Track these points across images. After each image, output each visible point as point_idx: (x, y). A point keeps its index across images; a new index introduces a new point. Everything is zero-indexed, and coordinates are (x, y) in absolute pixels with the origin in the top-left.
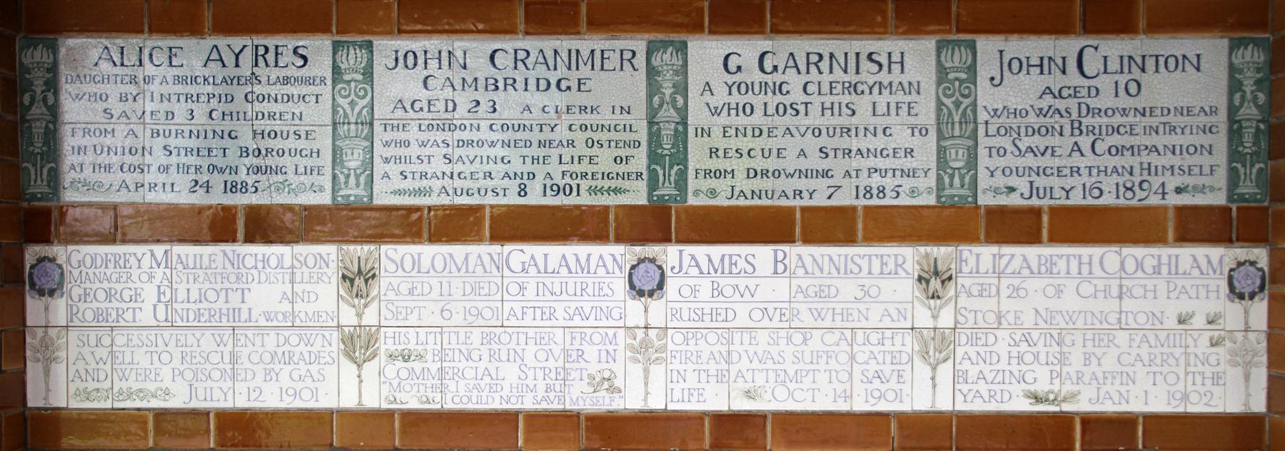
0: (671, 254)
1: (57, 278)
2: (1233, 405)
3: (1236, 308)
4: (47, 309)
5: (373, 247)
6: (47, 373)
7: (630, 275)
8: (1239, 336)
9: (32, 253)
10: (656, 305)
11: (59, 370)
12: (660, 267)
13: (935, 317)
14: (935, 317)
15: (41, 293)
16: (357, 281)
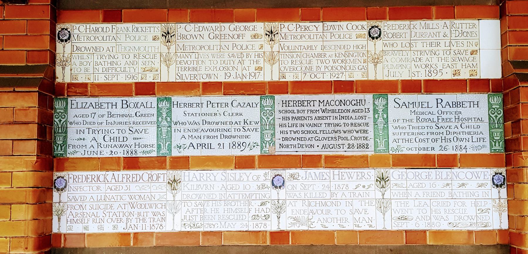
0: (286, 173)
1: (64, 184)
2: (496, 227)
3: (495, 190)
4: (60, 195)
5: (179, 172)
6: (59, 219)
7: (272, 180)
8: (497, 201)
9: (56, 174)
10: (282, 191)
11: (63, 219)
12: (283, 178)
13: (383, 195)
14: (383, 195)
15: (58, 190)
16: (174, 182)
